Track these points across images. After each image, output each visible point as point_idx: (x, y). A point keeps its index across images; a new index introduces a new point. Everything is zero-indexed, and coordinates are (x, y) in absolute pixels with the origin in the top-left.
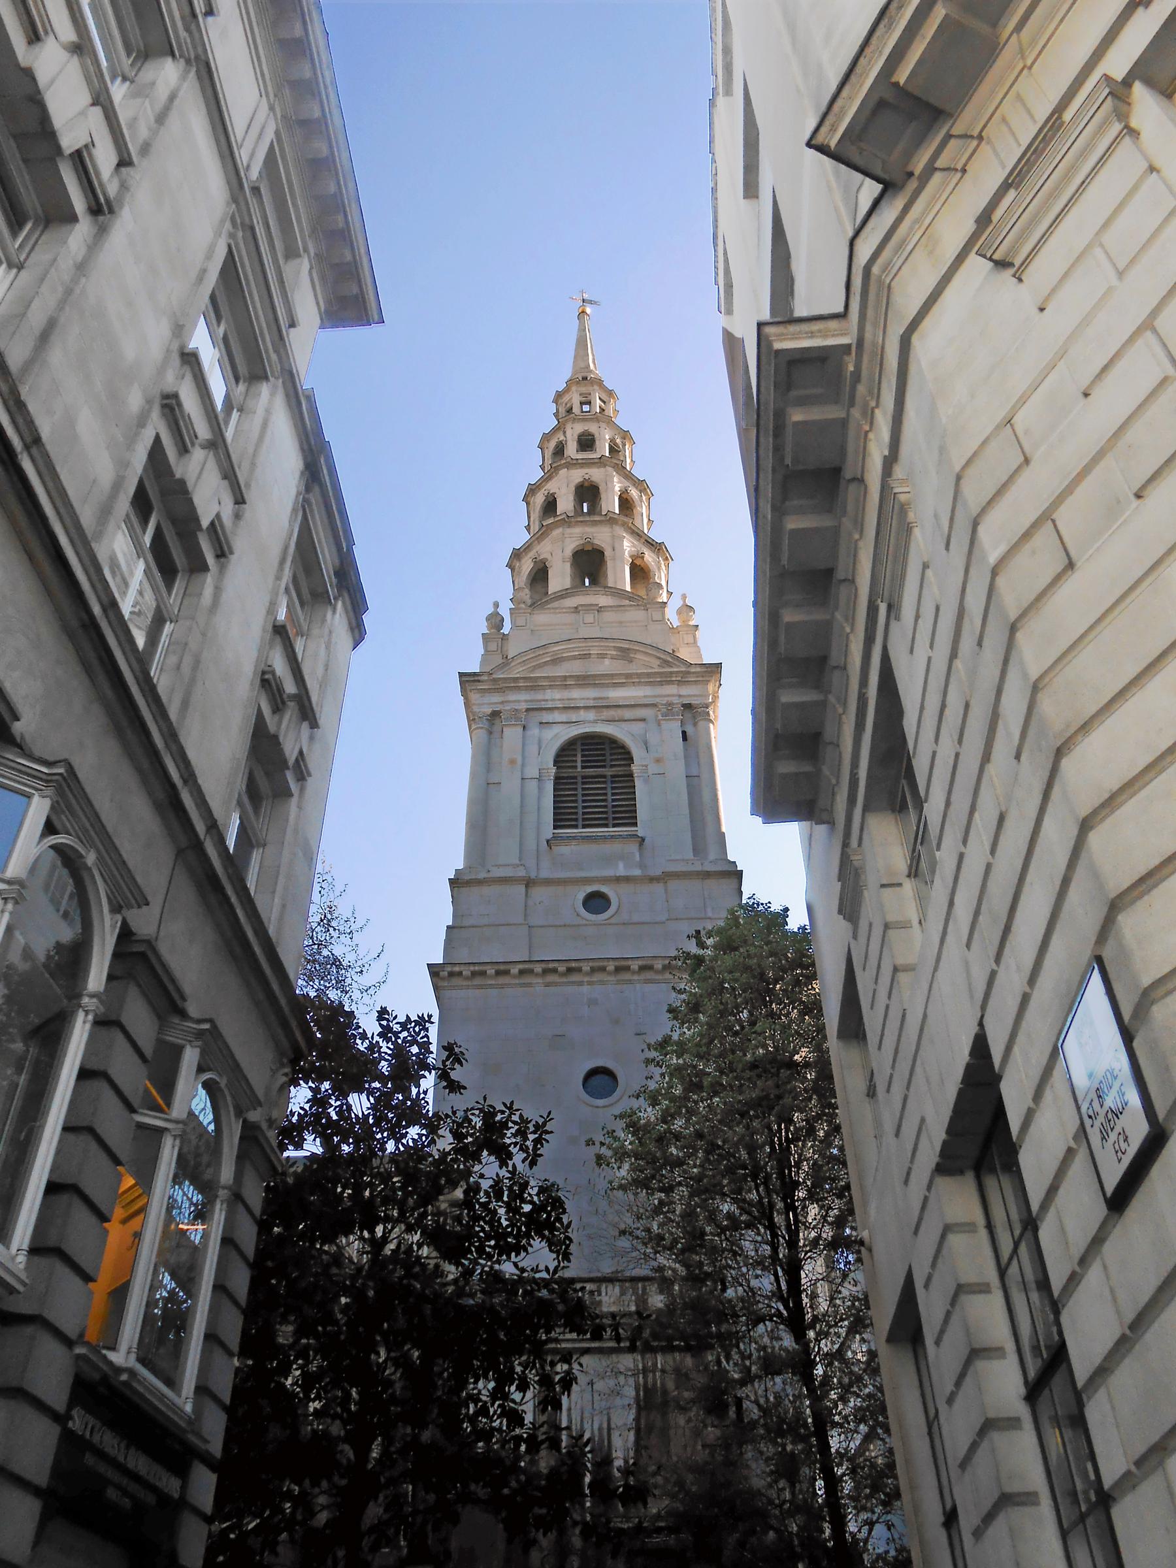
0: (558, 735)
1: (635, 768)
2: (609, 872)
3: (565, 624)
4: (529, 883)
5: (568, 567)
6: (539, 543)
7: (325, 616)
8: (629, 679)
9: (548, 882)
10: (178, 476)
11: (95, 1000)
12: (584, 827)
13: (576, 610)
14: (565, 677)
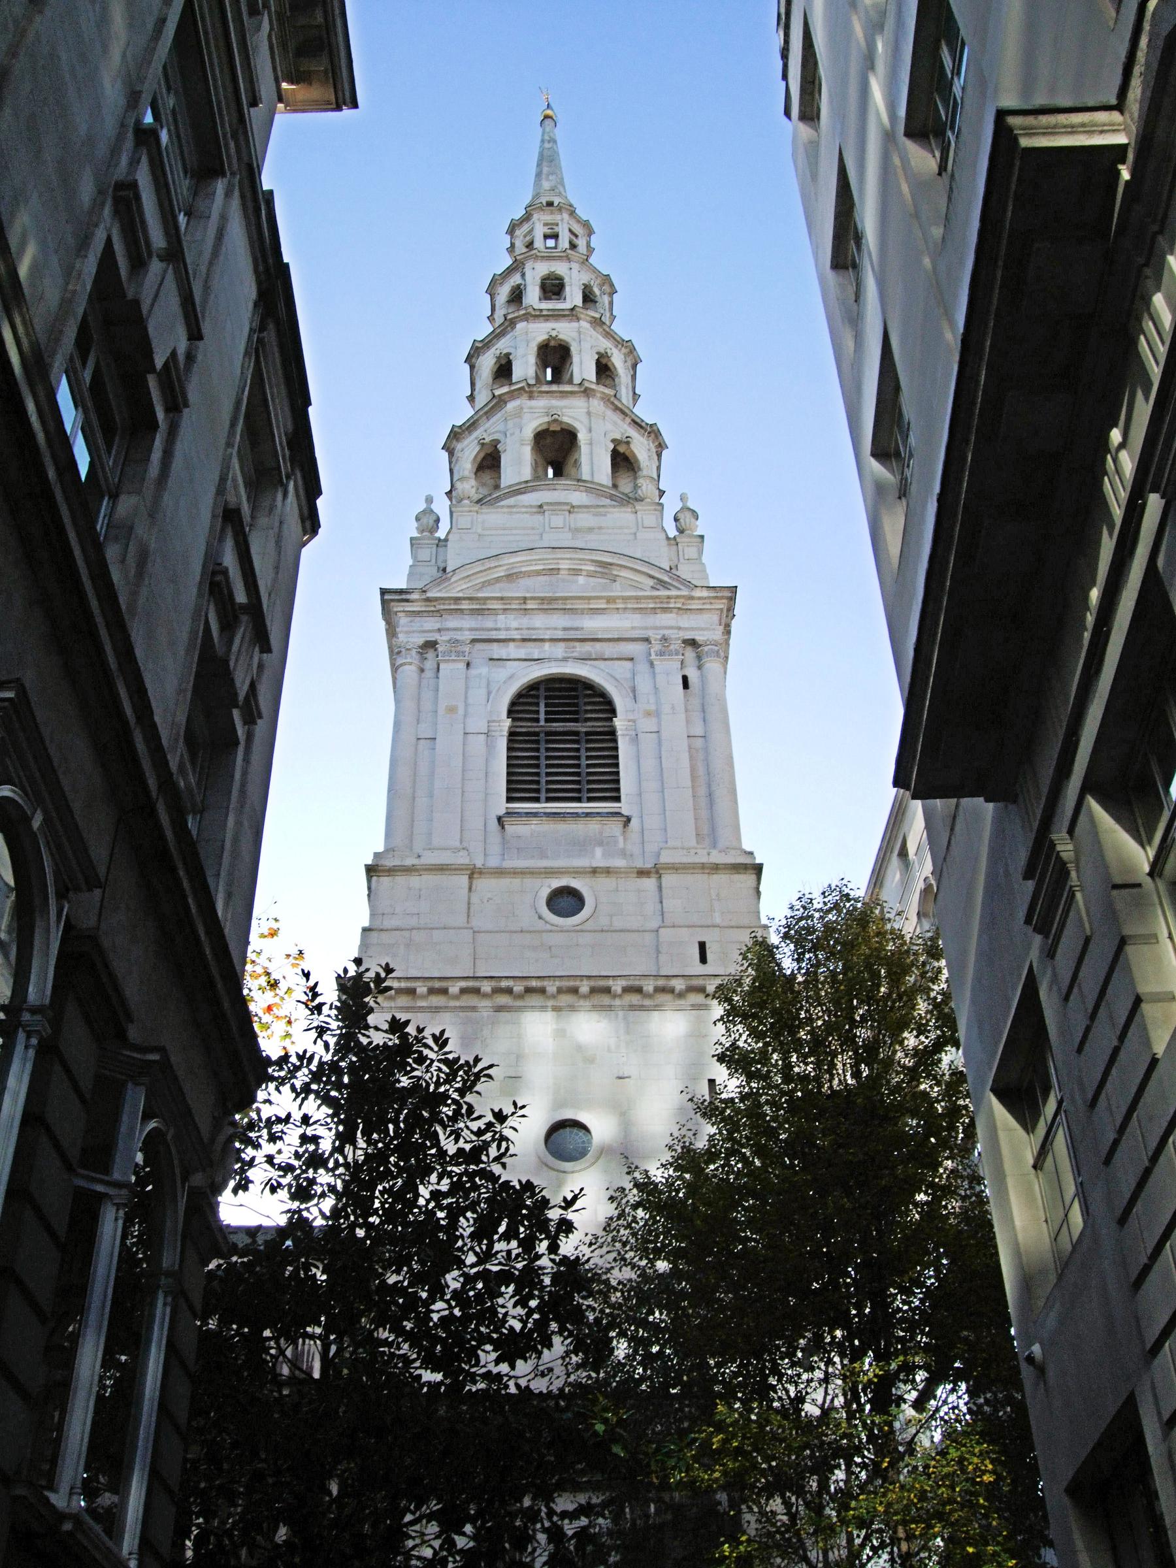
1: (618, 723)
4: (473, 873)
5: (527, 453)
6: (488, 419)
7: (274, 500)
9: (500, 872)
10: (130, 295)
11: (38, 1017)
12: (548, 800)
14: (525, 598)
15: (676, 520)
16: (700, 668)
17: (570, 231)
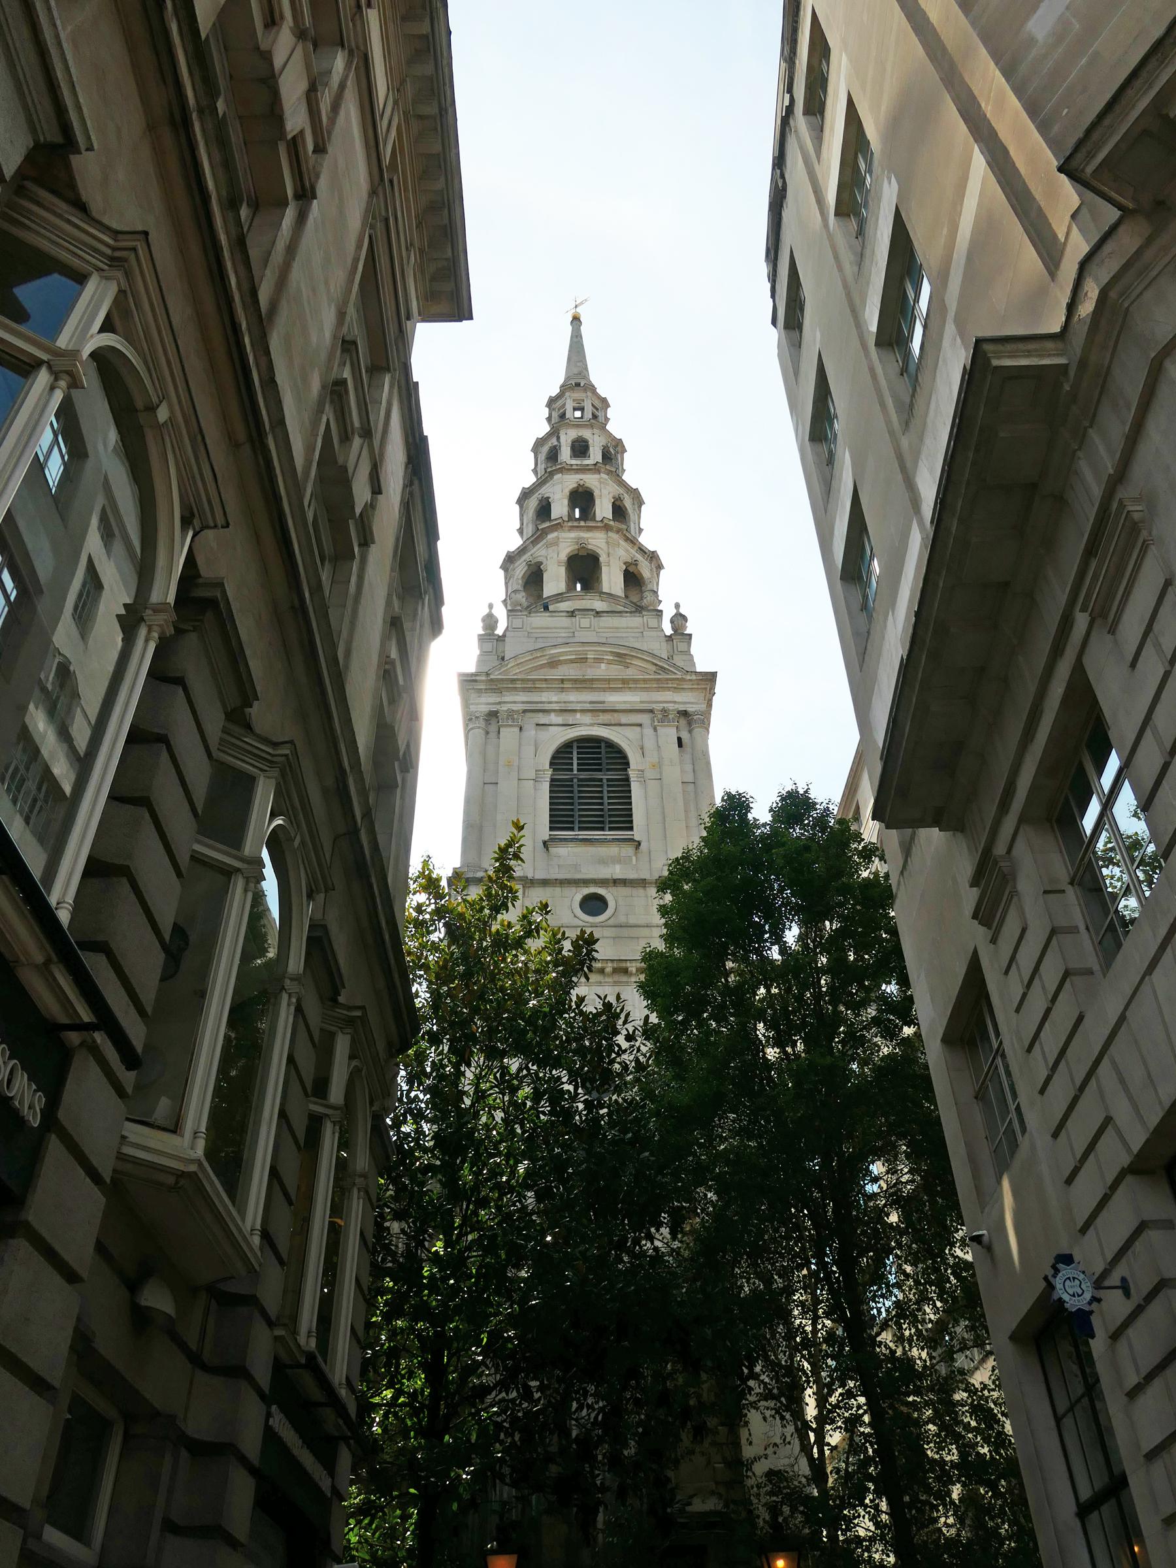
0: (558, 737)
1: (632, 773)
2: (605, 873)
3: (563, 628)
5: (562, 571)
7: (416, 609)
8: (626, 684)
10: (341, 461)
12: (580, 829)
13: (572, 614)
15: (672, 621)
16: (690, 732)
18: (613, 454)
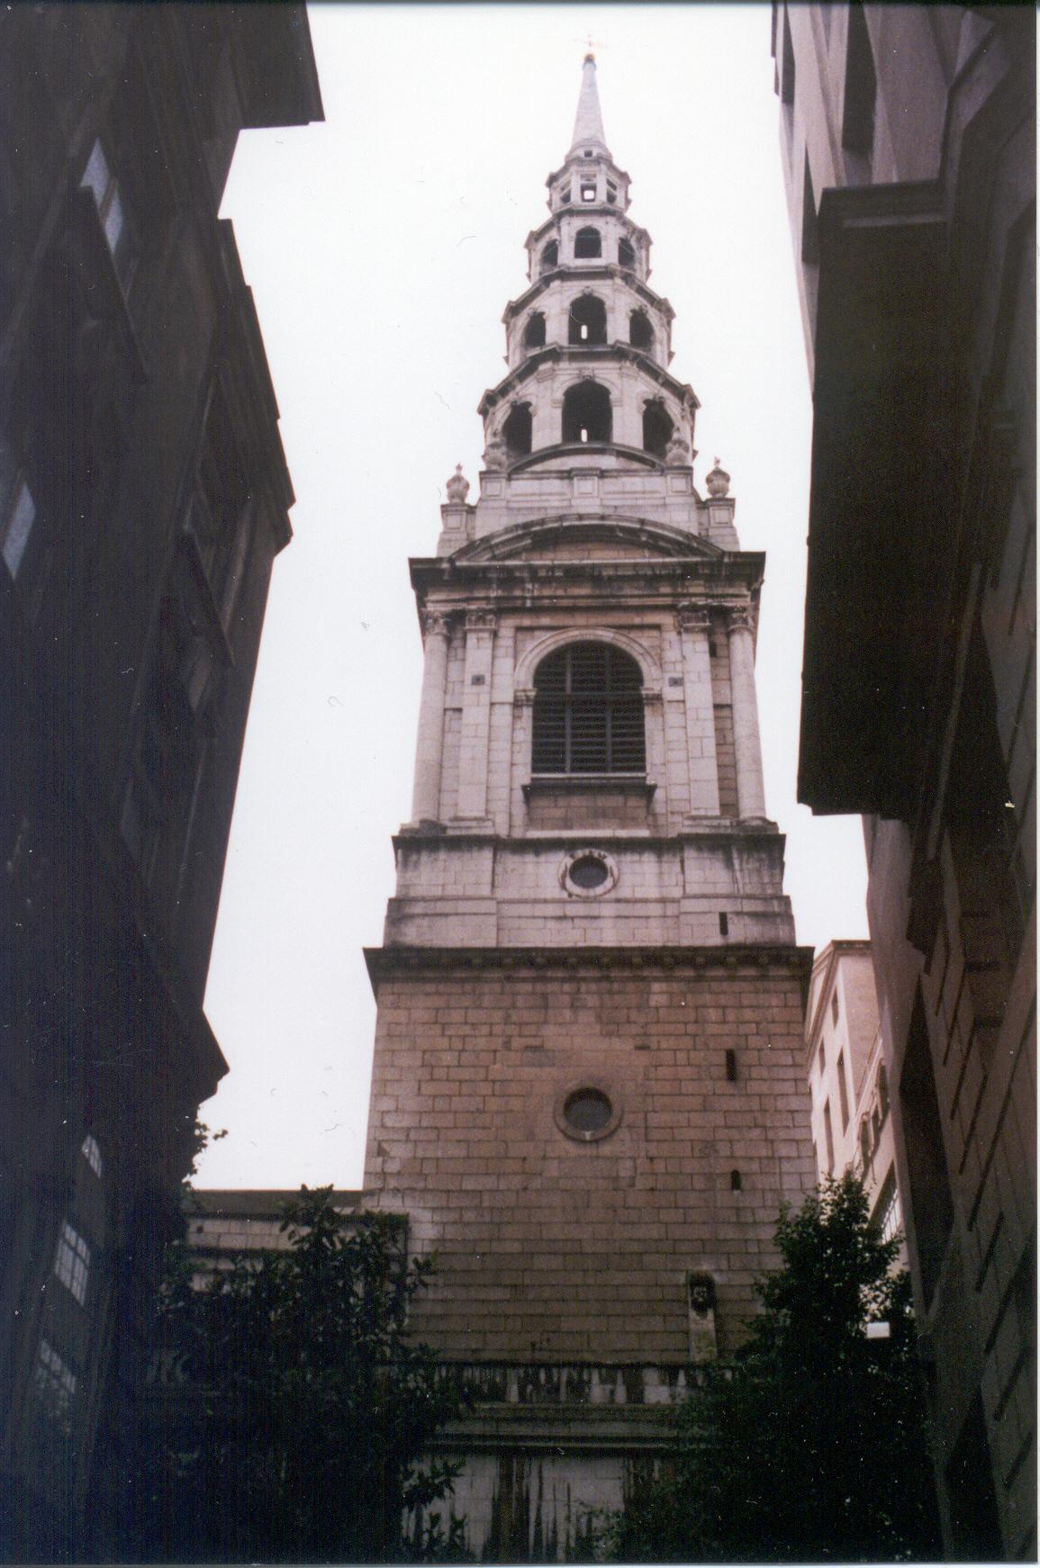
4: (500, 845)
5: (558, 413)
13: (568, 475)
15: (709, 480)
17: (609, 183)
18: (633, 247)
